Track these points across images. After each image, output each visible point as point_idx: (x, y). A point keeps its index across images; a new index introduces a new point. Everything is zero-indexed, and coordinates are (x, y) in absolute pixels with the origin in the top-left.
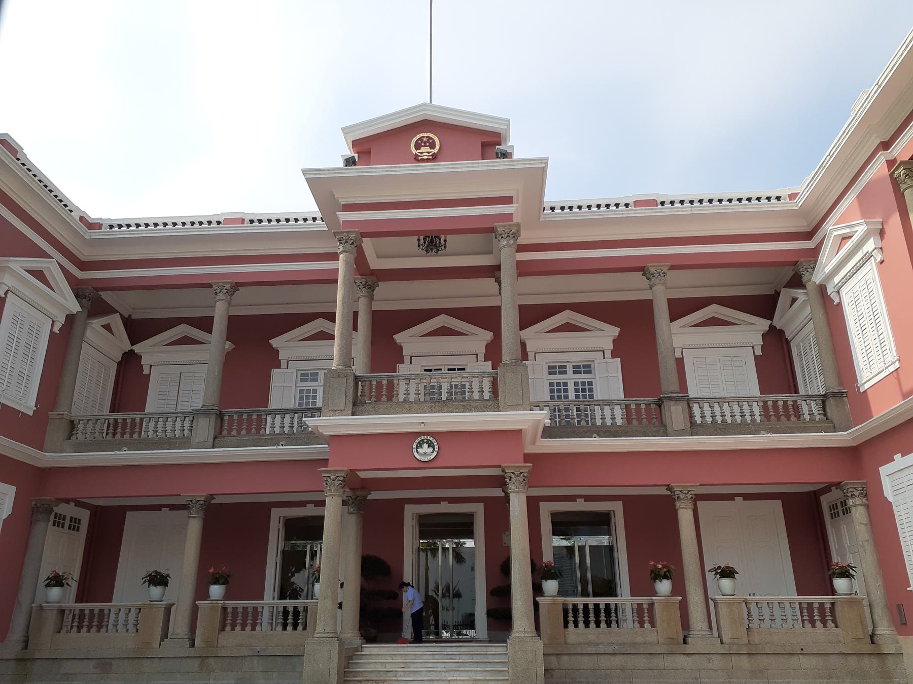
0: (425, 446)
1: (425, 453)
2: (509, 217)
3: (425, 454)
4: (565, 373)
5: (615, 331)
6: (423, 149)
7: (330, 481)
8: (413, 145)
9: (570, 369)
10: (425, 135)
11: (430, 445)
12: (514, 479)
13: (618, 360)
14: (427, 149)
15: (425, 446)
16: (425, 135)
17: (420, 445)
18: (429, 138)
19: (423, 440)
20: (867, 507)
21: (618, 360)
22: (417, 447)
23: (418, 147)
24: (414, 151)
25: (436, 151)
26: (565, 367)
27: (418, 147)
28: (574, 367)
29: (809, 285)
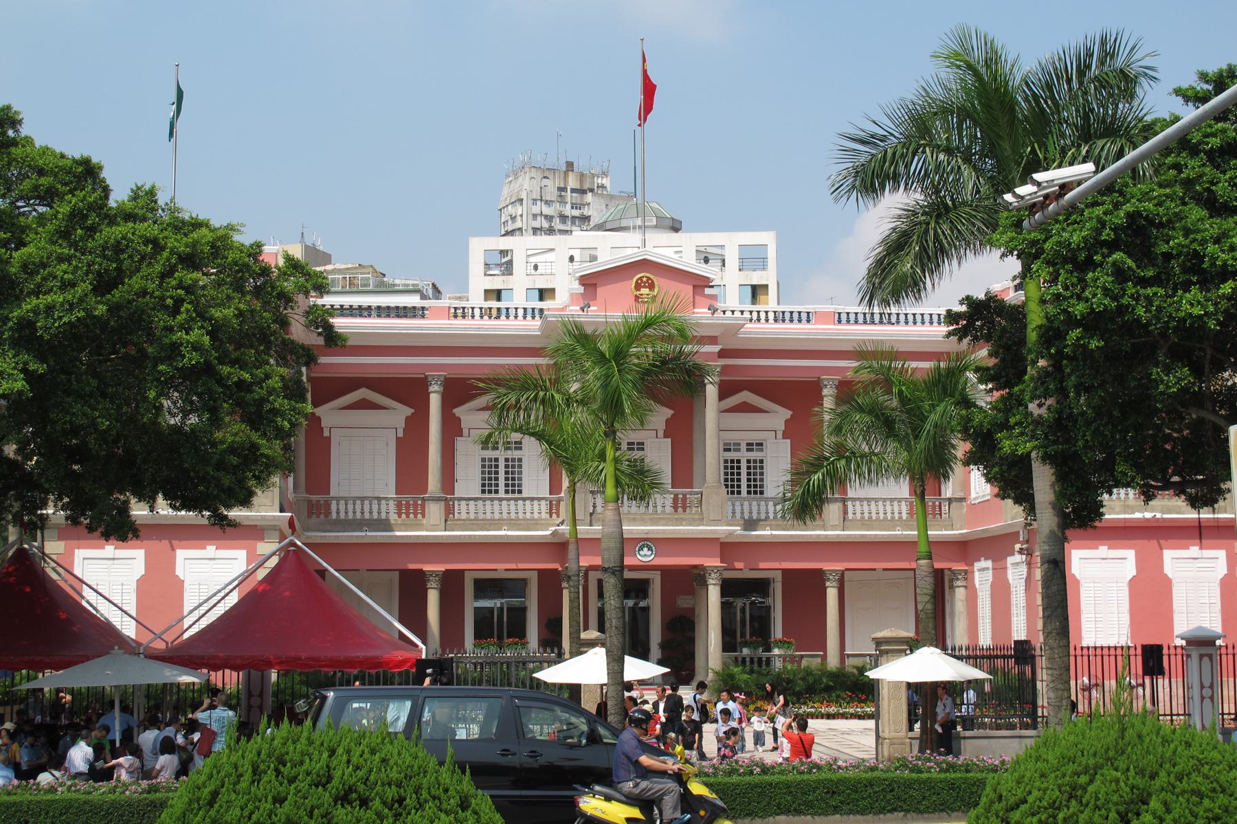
0: (645, 549)
3: (646, 555)
4: (739, 450)
5: (787, 414)
9: (743, 447)
10: (648, 275)
13: (788, 441)
16: (648, 275)
18: (649, 278)
19: (643, 545)
21: (788, 441)
22: (639, 550)
23: (638, 287)
26: (739, 444)
27: (638, 287)
28: (748, 444)
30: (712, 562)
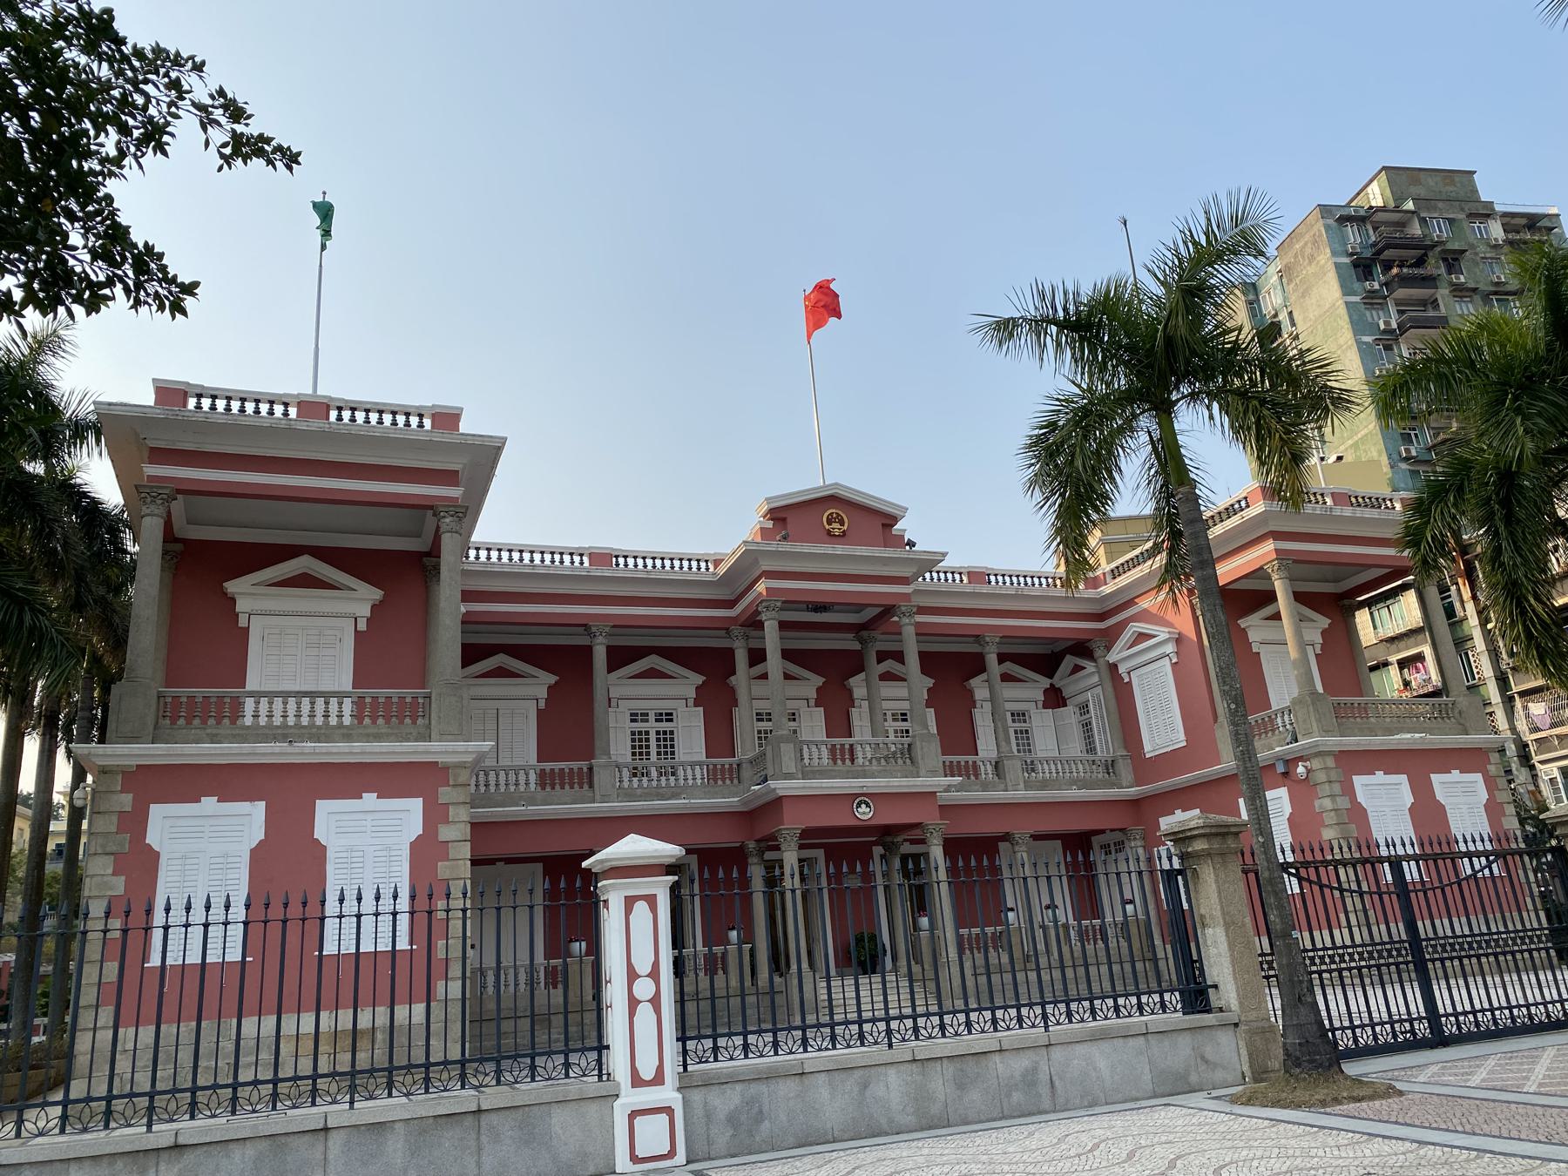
1: (864, 813)
2: (906, 596)
6: (834, 525)
7: (789, 838)
8: (825, 519)
11: (868, 805)
12: (935, 834)
14: (838, 526)
15: (863, 806)
17: (859, 805)
18: (838, 515)
20: (1144, 847)
23: (829, 523)
24: (827, 527)
25: (845, 528)
27: (829, 523)
29: (1101, 661)
30: (930, 817)
